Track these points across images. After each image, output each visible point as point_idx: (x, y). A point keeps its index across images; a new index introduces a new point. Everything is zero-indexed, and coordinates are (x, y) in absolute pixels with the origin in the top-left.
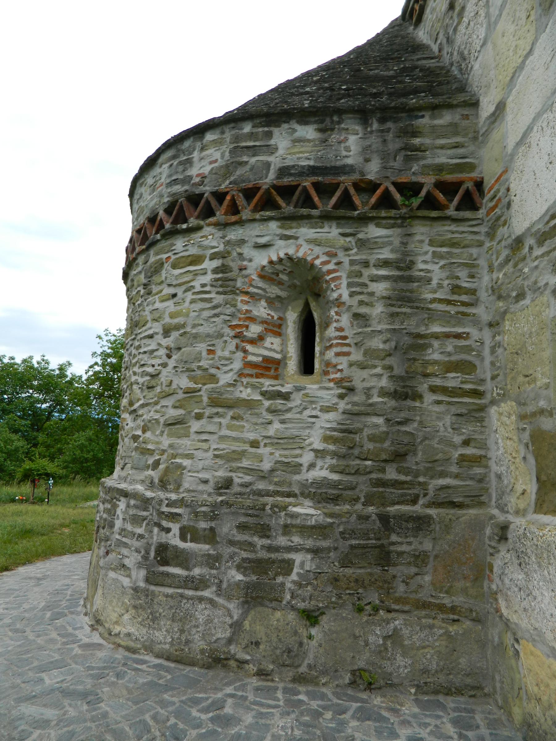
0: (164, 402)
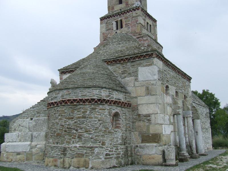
0: (100, 132)
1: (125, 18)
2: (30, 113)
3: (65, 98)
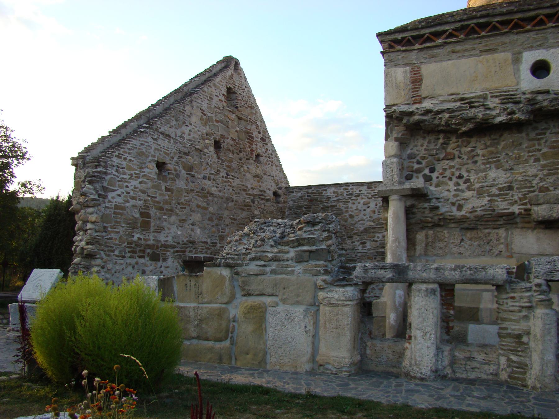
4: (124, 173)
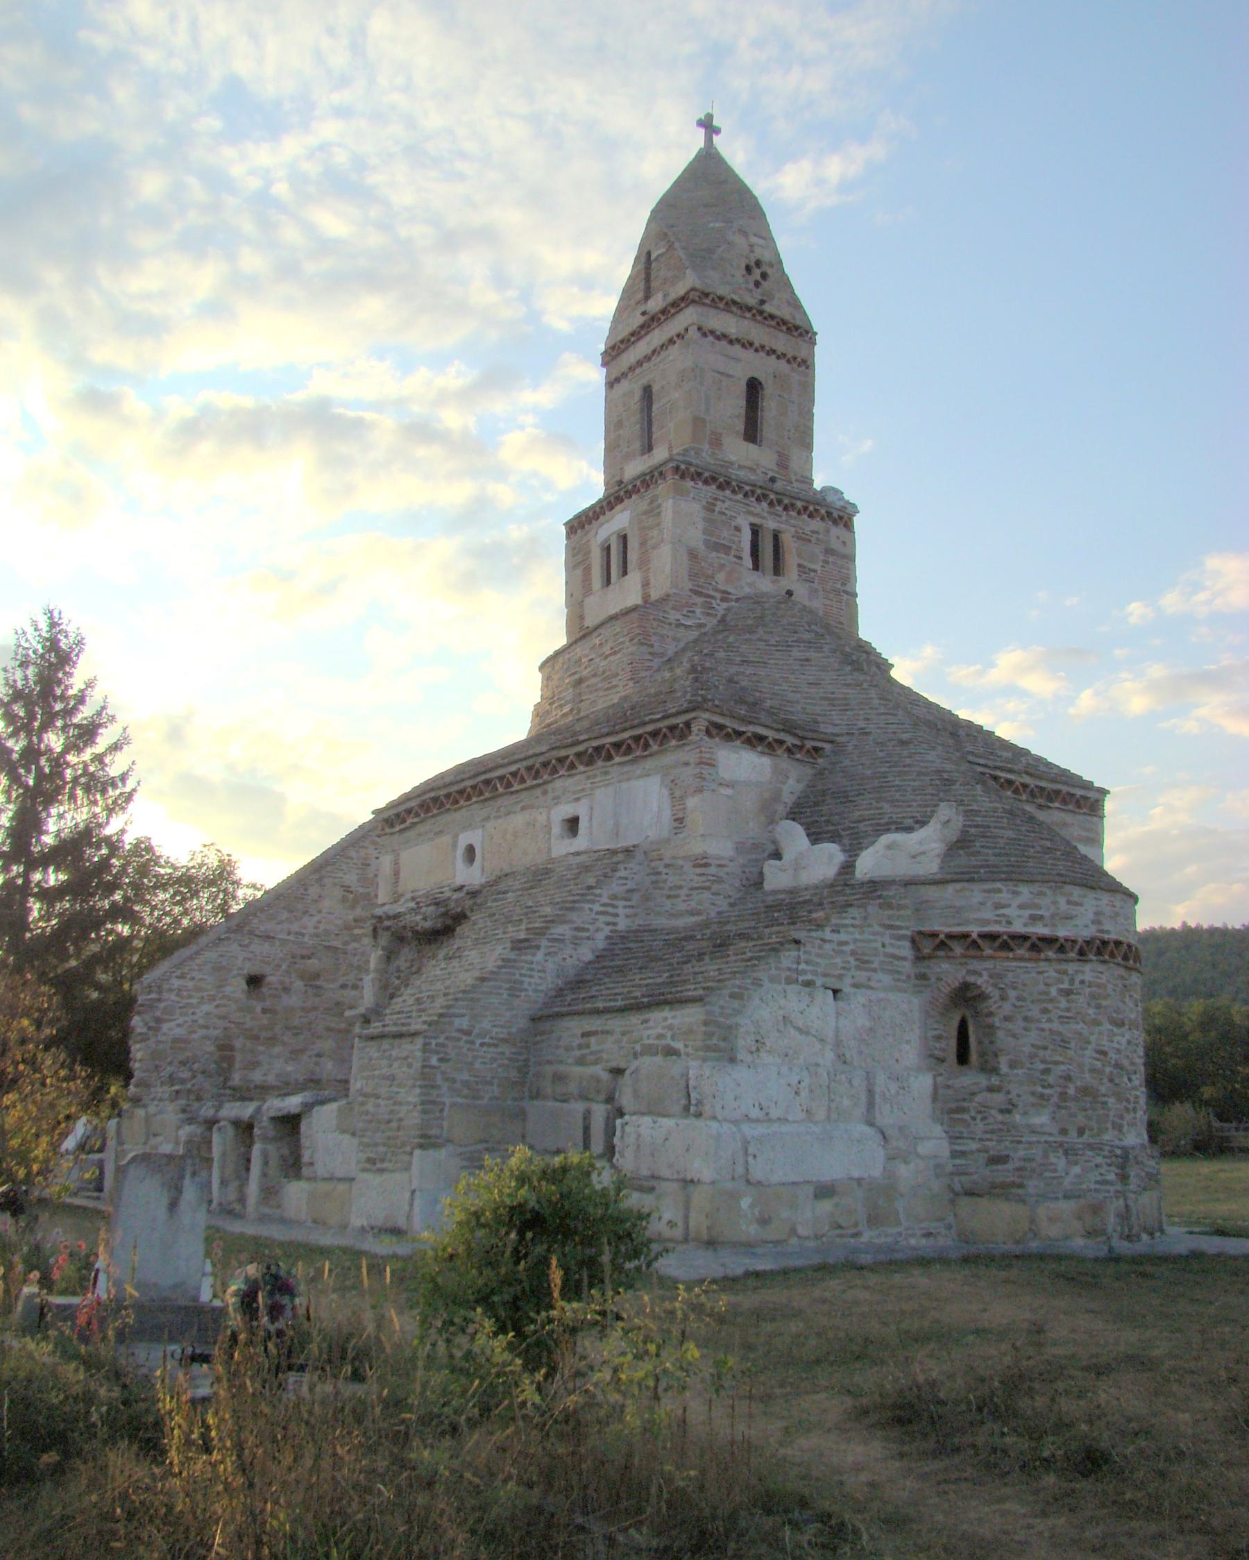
1: (798, 537)
2: (818, 955)
3: (1108, 932)
4: (190, 997)
